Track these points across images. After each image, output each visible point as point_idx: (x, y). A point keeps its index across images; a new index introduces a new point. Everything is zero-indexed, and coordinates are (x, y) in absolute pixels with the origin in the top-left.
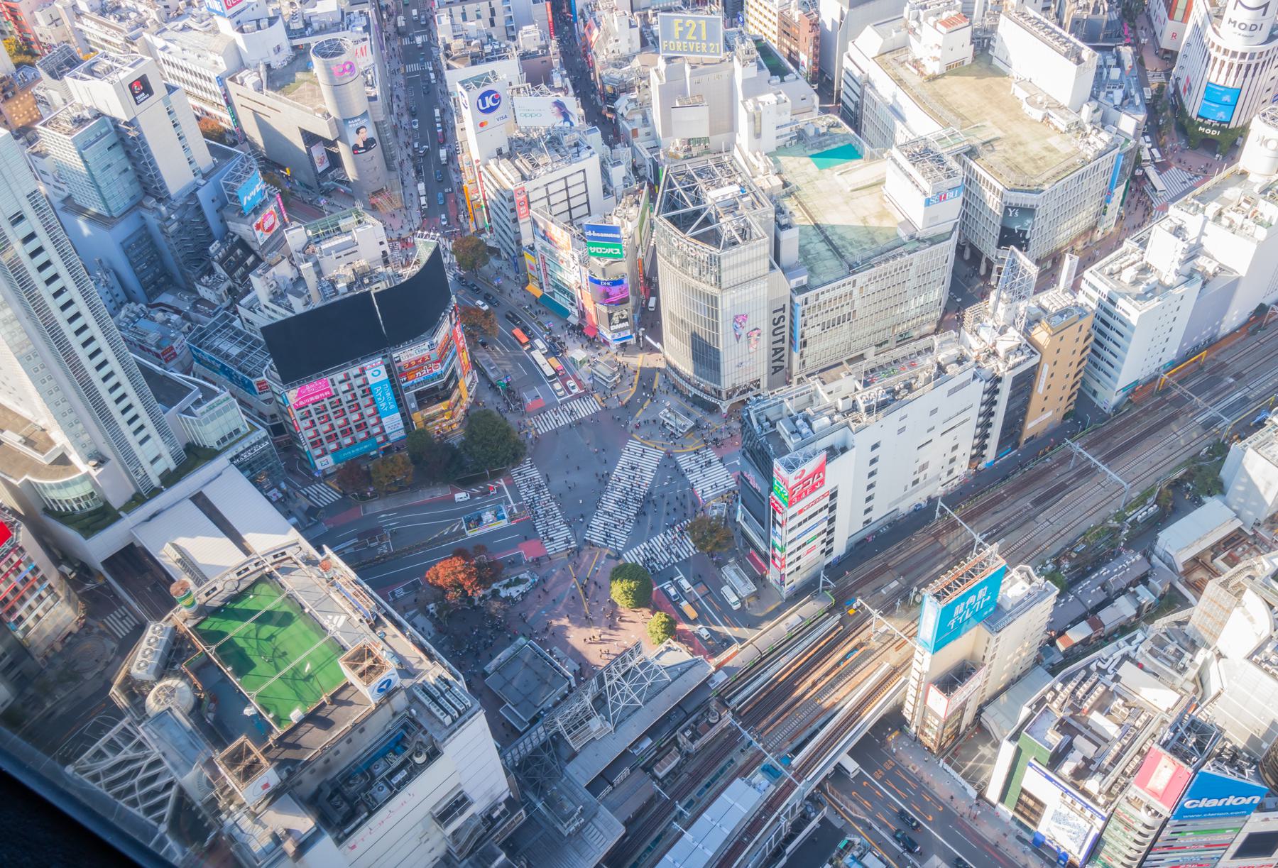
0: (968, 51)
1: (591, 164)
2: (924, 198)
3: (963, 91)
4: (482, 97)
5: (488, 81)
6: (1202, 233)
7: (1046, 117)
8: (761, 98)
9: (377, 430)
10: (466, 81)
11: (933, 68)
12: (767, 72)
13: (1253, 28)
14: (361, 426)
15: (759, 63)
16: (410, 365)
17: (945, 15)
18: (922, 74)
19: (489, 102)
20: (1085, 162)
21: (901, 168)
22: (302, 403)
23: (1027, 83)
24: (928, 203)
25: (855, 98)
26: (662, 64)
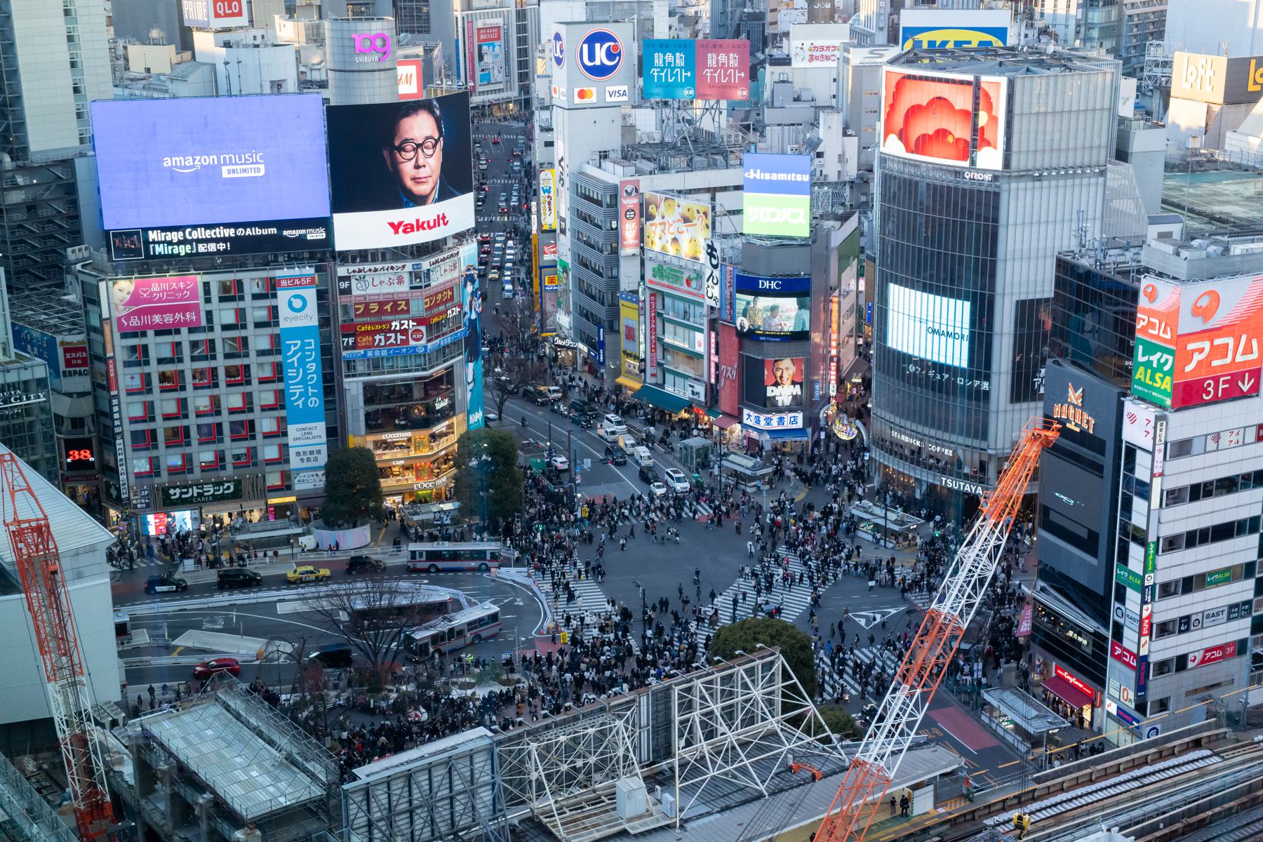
9: (271, 452)
14: (246, 430)
16: (367, 312)
22: (135, 322)
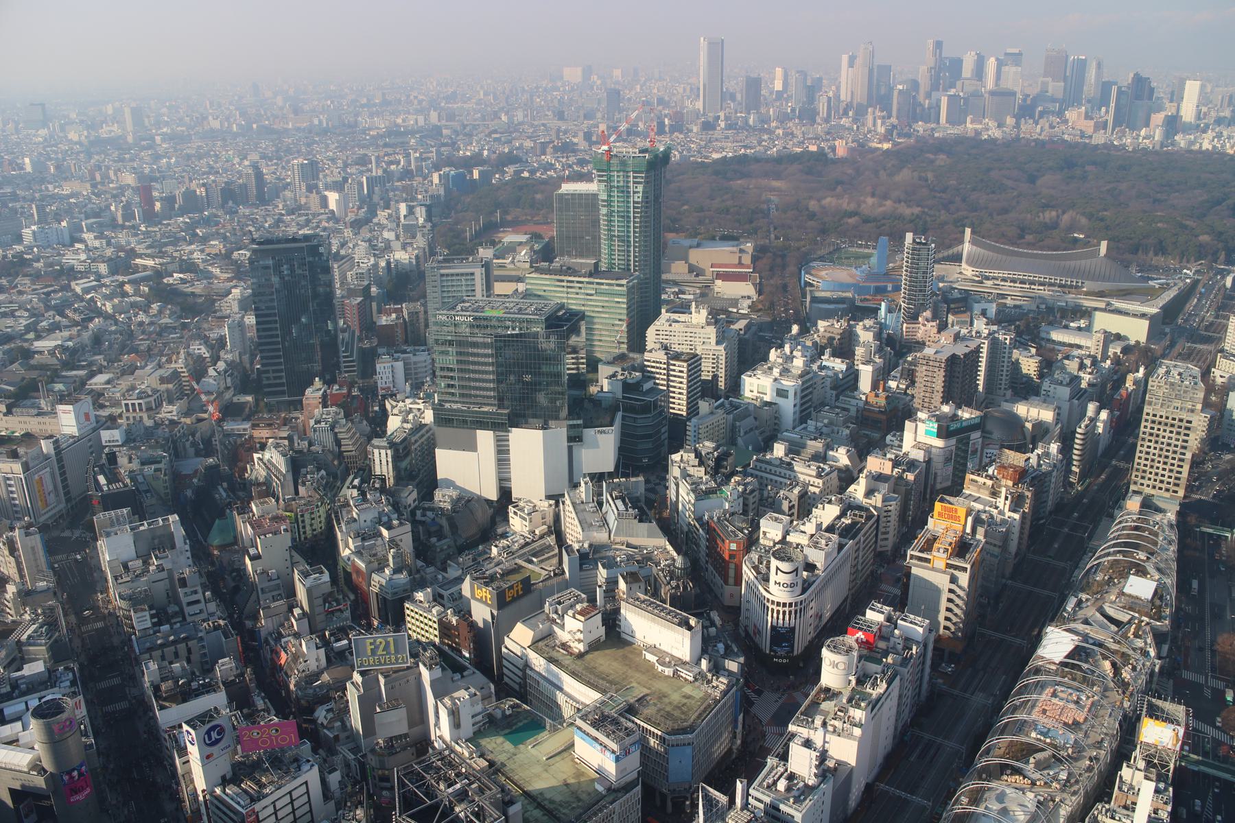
0: (602, 631)
1: (312, 775)
2: (613, 756)
3: (606, 662)
4: (208, 733)
5: (211, 716)
6: (825, 742)
7: (676, 672)
8: (456, 695)
10: (192, 720)
11: (579, 647)
12: (449, 672)
13: (792, 585)
15: (442, 666)
17: (578, 607)
18: (571, 654)
19: (214, 735)
20: (717, 702)
21: (588, 734)
23: (653, 649)
24: (617, 759)
25: (518, 680)
26: (357, 678)
